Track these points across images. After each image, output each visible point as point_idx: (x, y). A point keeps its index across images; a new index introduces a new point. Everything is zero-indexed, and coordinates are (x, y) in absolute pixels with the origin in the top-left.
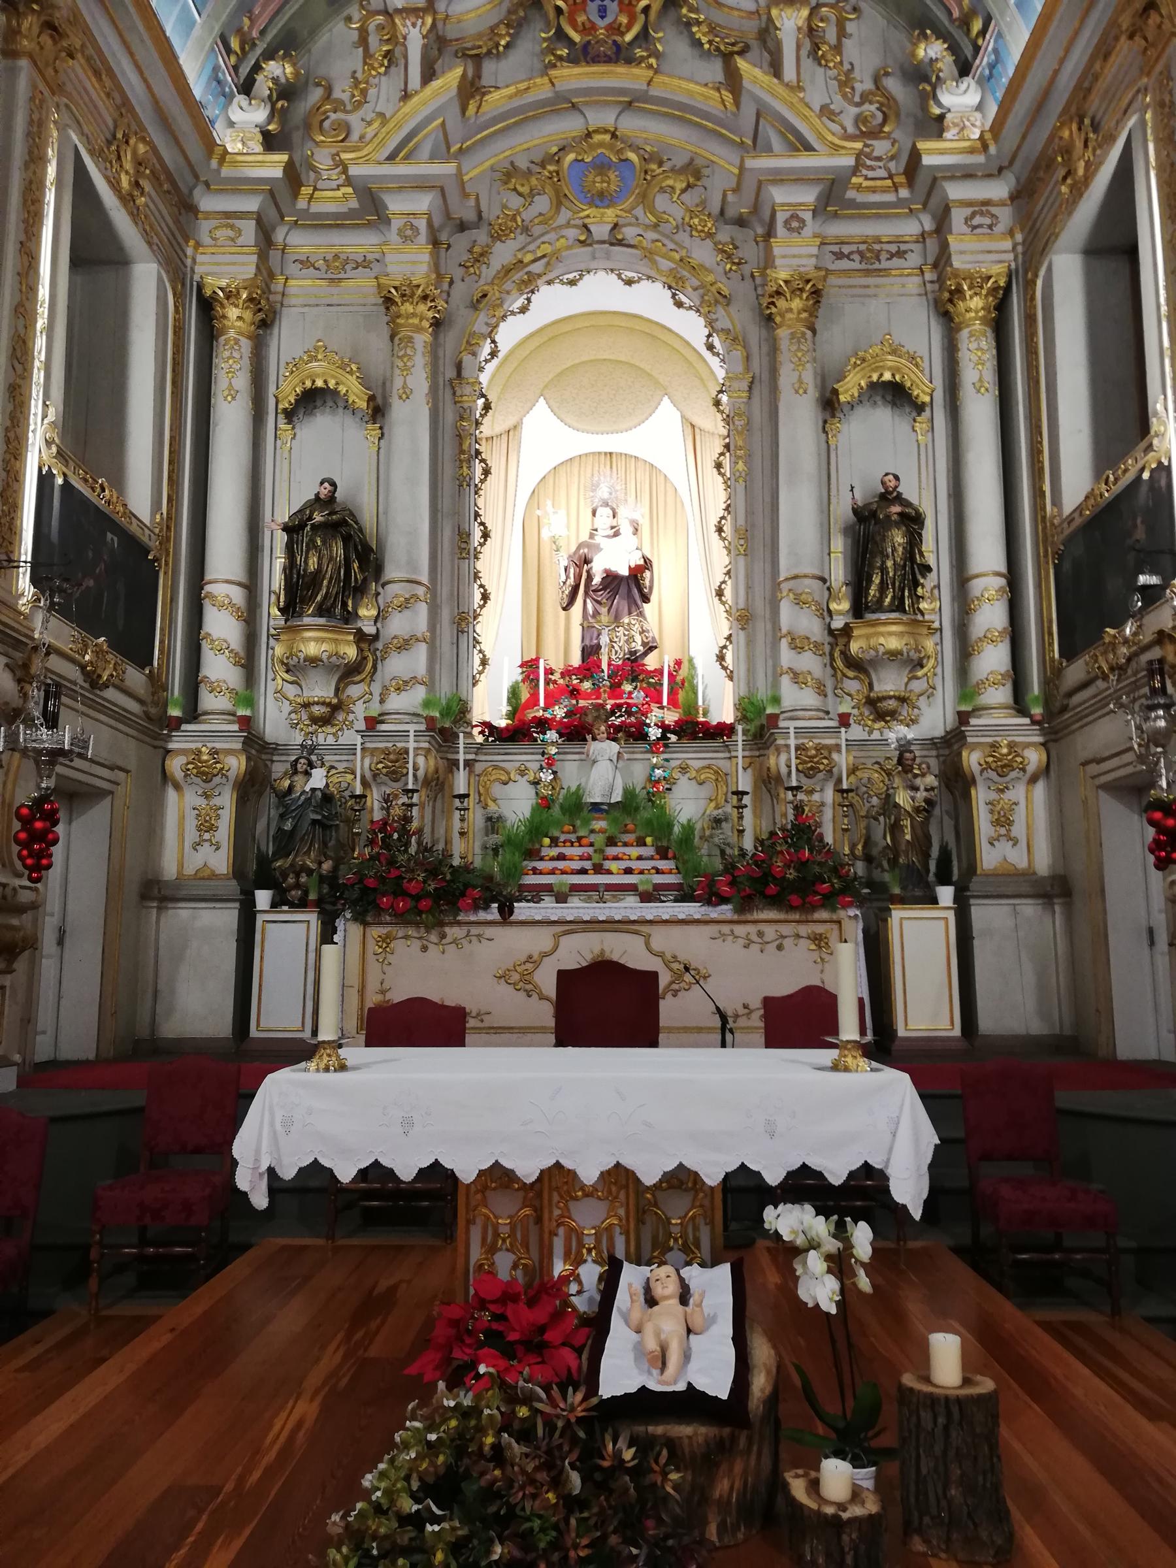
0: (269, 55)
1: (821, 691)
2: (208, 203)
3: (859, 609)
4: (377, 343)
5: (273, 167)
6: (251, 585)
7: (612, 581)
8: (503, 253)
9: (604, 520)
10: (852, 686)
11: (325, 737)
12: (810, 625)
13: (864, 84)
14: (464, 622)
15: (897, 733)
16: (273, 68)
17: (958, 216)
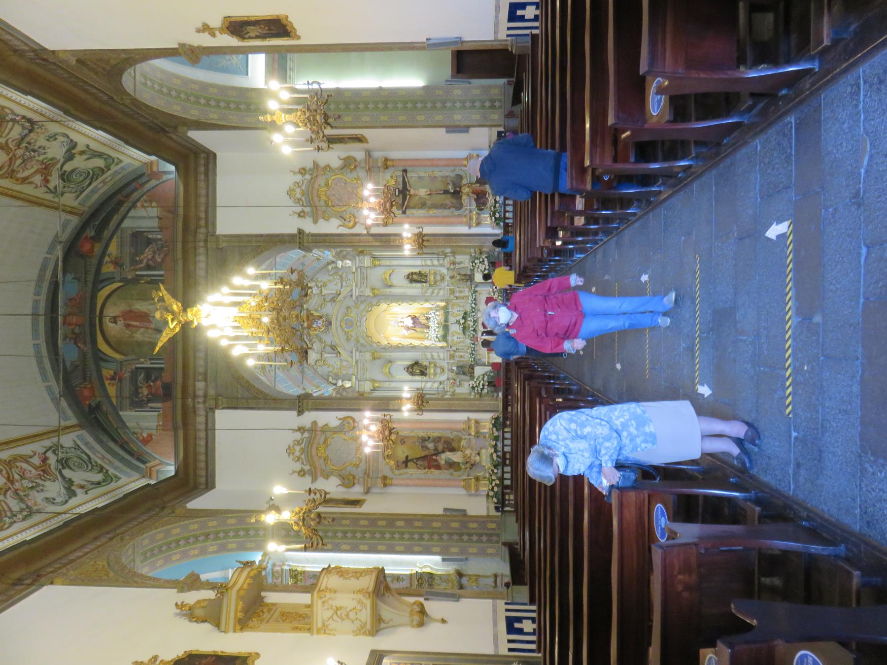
0: (328, 381)
1: (440, 289)
2: (357, 390)
3: (426, 282)
4: (378, 362)
5: (354, 378)
6: (422, 382)
7: (414, 323)
8: (362, 341)
9: (400, 324)
10: (438, 283)
11: (446, 370)
12: (430, 291)
13: (331, 278)
14: (426, 347)
15: (447, 278)
16: (331, 379)
17: (361, 265)
